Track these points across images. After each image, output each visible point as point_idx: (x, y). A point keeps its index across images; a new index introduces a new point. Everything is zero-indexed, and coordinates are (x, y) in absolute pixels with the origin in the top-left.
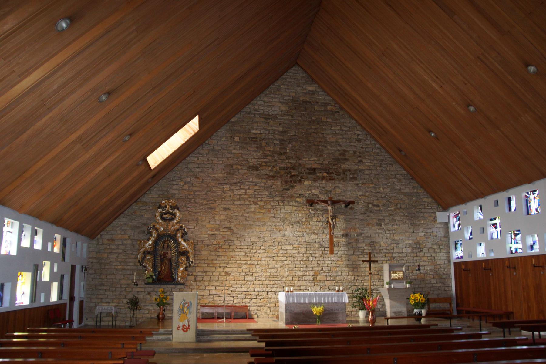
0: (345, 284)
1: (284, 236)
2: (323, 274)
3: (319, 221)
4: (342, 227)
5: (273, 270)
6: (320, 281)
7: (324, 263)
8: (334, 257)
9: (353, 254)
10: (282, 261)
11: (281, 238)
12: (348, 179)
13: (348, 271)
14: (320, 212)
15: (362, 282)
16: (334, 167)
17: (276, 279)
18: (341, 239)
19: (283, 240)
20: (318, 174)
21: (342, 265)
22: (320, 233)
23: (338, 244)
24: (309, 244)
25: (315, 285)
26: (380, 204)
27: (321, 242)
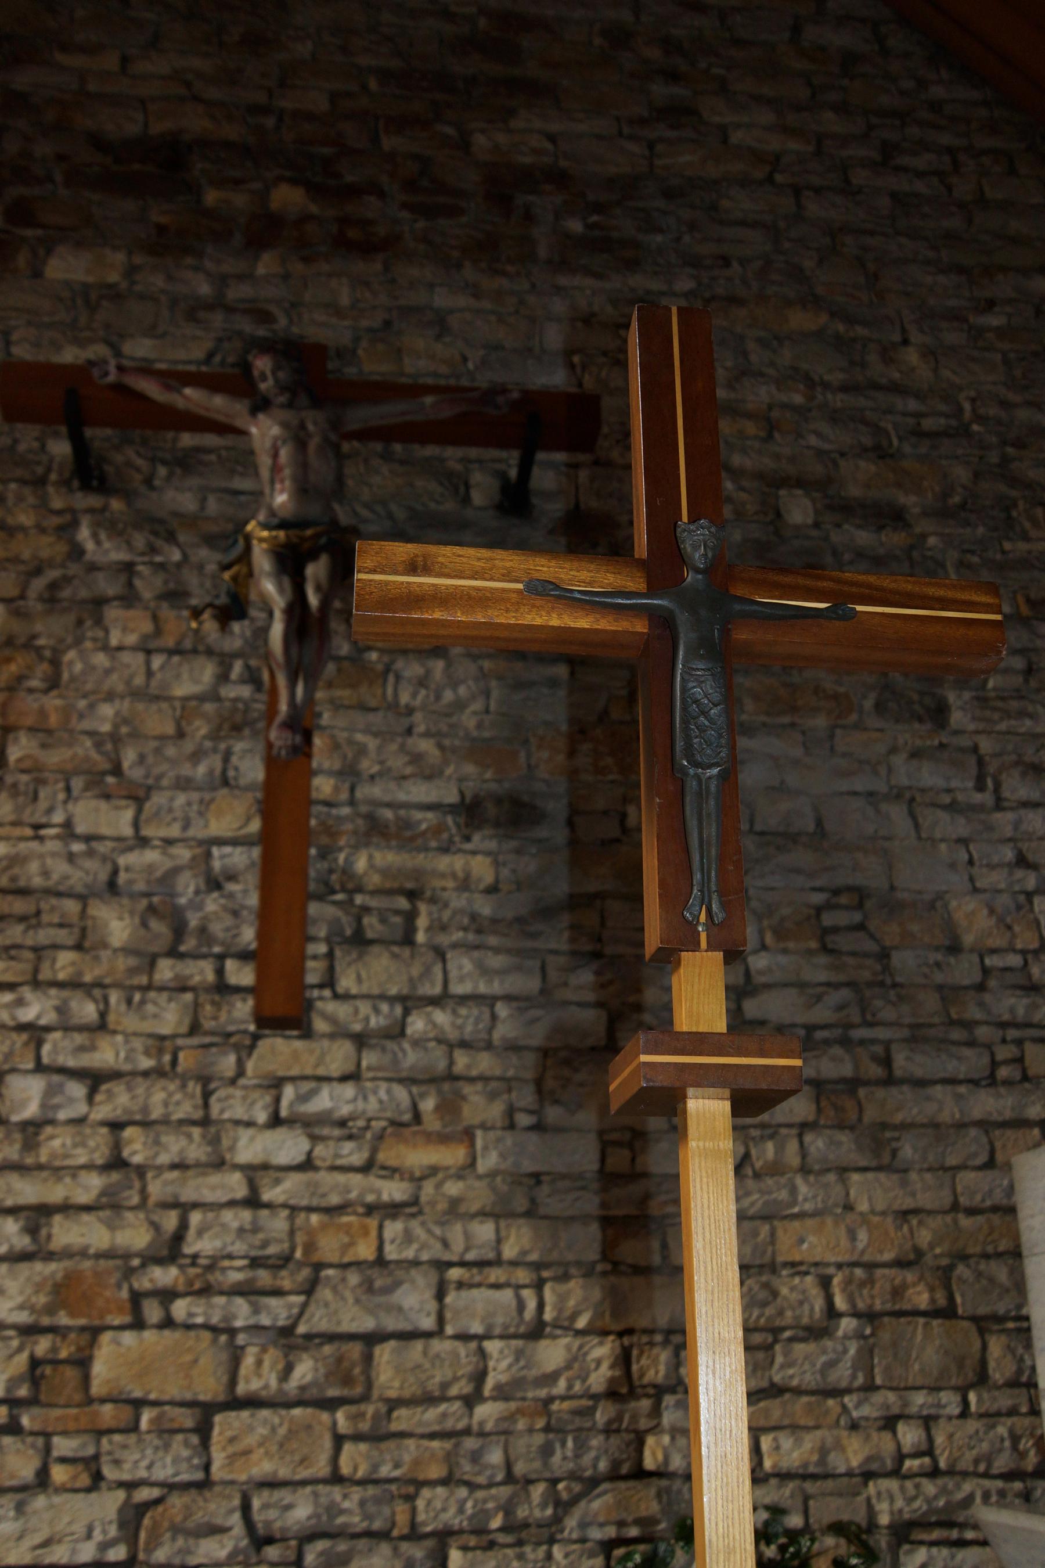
0: (495, 1457)
2: (180, 1308)
3: (176, 651)
4: (468, 720)
6: (139, 1404)
7: (197, 1151)
8: (352, 1077)
12: (542, 252)
14: (204, 553)
16: (388, 143)
18: (443, 863)
20: (211, 197)
21: (453, 1188)
22: (183, 784)
23: (410, 917)
25: (59, 1474)
26: (908, 500)
27: (187, 886)
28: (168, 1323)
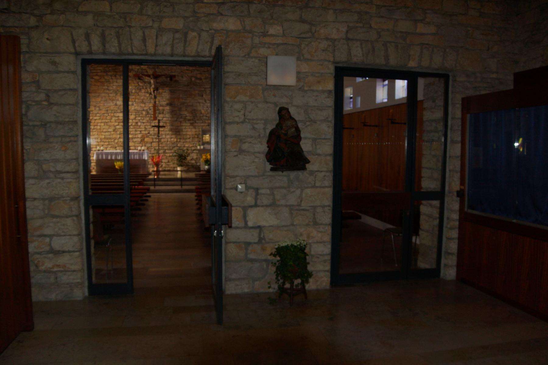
1: (116, 105)
4: (167, 97)
5: (107, 134)
9: (176, 120)
10: (115, 126)
11: (114, 107)
13: (172, 135)
15: (184, 143)
17: (110, 141)
19: (115, 109)
22: (148, 103)
24: (137, 111)
26: (202, 78)
27: (148, 110)
28: (149, 137)
